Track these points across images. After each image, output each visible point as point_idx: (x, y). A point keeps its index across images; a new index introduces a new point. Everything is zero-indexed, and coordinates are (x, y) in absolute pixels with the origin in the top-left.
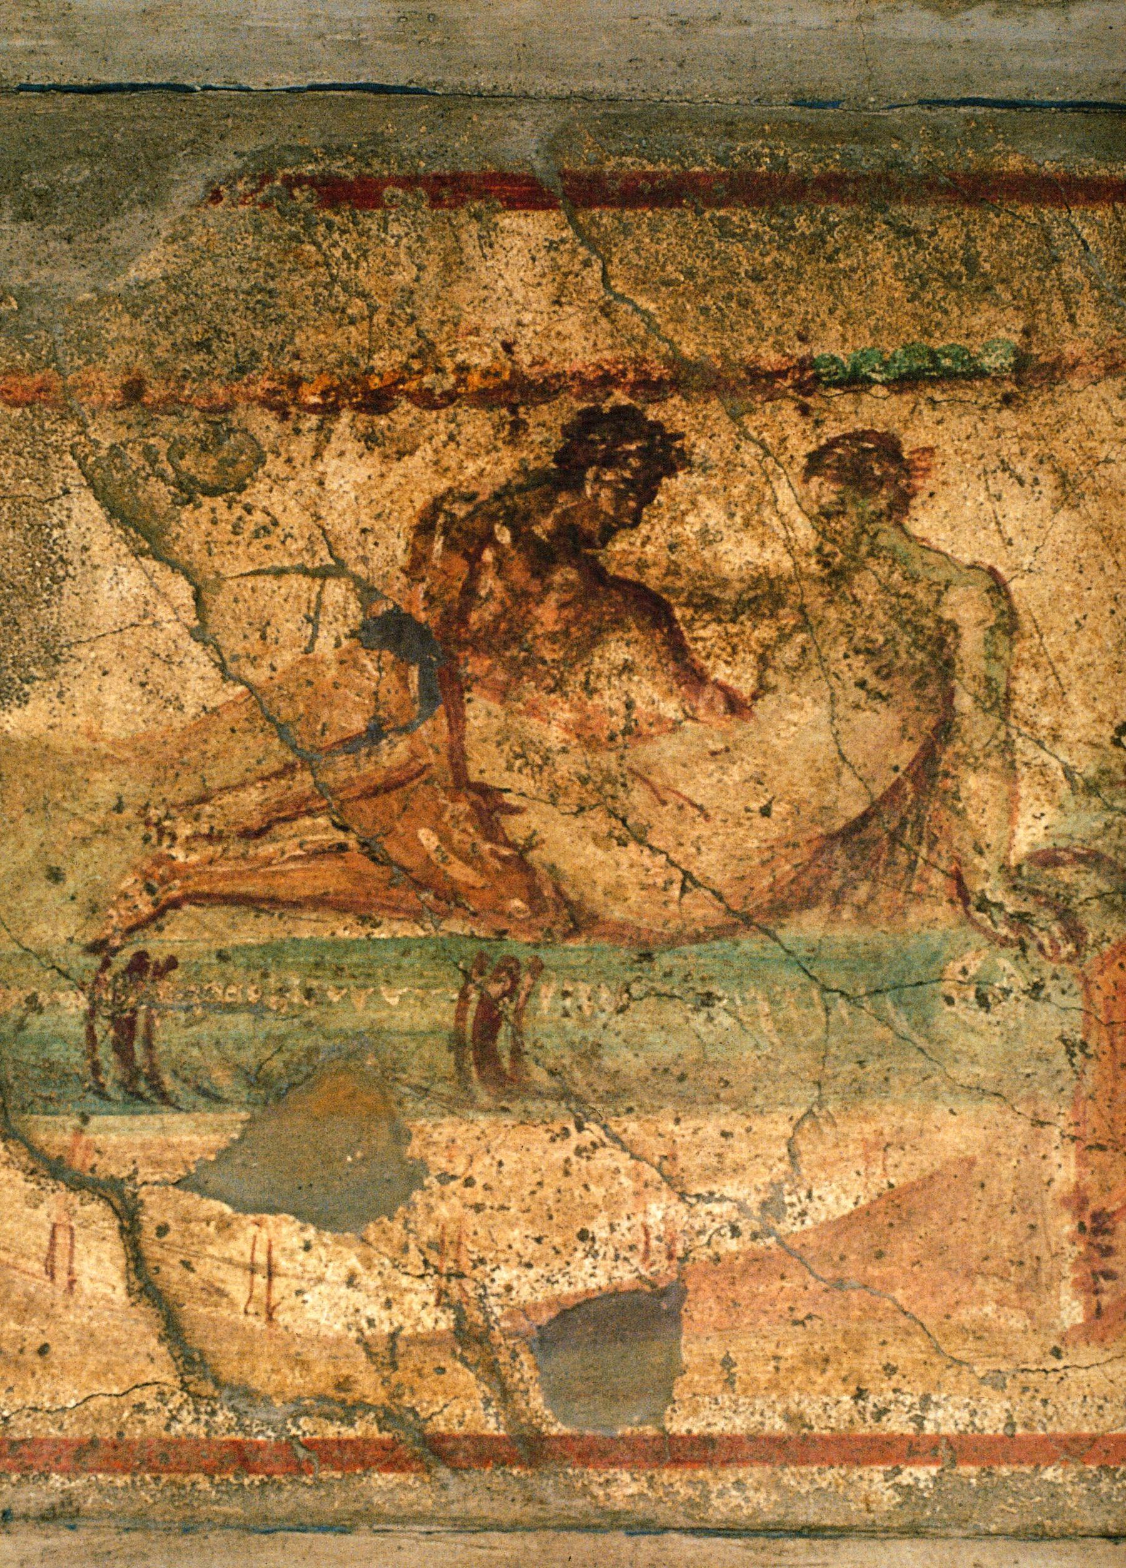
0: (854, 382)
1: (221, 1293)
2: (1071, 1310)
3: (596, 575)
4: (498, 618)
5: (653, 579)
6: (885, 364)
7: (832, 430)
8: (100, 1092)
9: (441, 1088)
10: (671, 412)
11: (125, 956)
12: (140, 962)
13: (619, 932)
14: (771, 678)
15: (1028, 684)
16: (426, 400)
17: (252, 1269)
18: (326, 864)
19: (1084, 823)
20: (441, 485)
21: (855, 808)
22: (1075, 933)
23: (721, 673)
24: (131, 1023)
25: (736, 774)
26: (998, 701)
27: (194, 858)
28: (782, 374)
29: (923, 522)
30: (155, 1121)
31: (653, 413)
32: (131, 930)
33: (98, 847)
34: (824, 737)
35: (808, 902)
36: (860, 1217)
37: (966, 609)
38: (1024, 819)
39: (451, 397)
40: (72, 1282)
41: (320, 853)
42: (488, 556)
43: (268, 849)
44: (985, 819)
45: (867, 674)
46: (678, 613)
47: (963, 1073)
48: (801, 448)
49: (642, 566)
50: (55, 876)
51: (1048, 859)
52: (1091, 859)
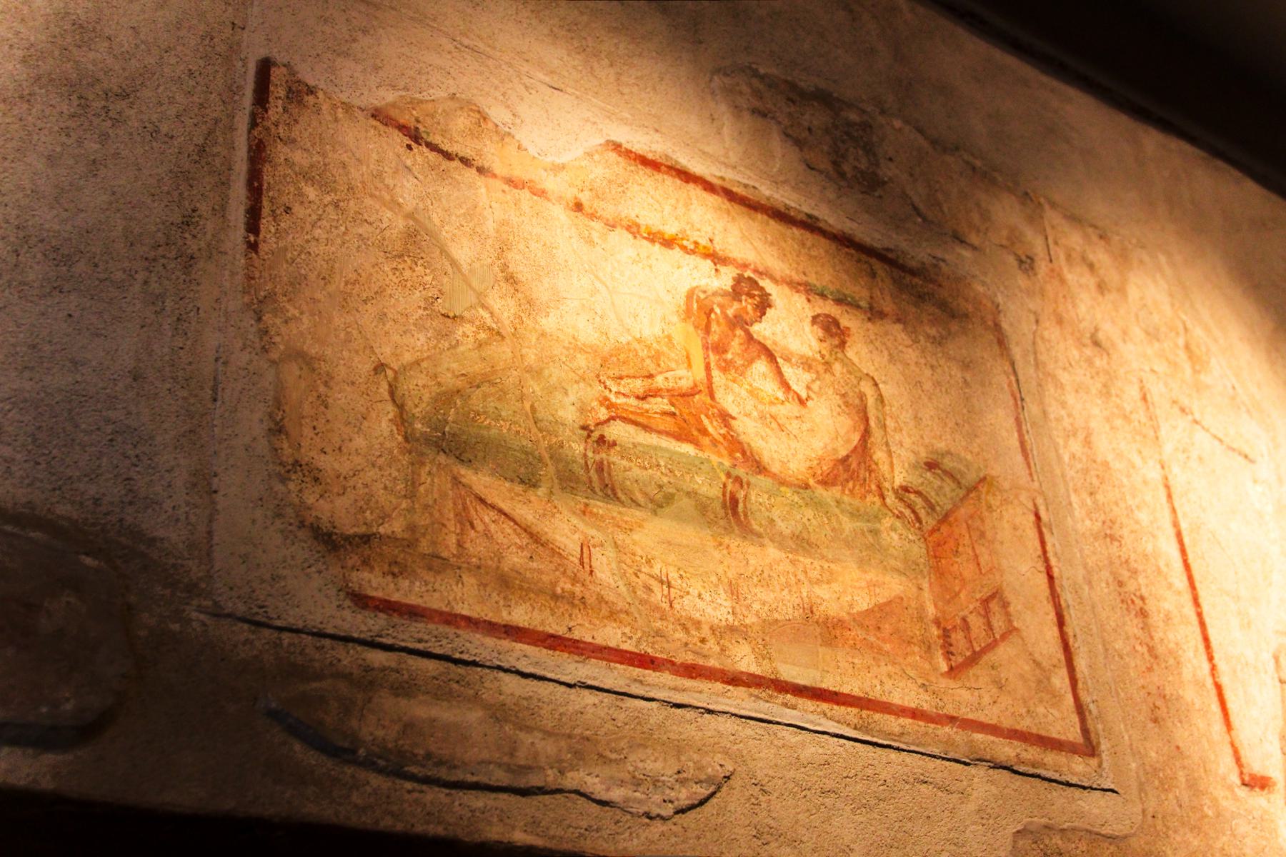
0: (823, 296)
1: (650, 590)
2: (944, 667)
3: (750, 337)
4: (720, 340)
5: (768, 343)
6: (832, 293)
7: (819, 311)
8: (593, 490)
9: (722, 523)
10: (766, 283)
11: (596, 435)
12: (602, 439)
13: (774, 476)
14: (811, 394)
15: (890, 423)
16: (684, 248)
17: (662, 582)
18: (668, 419)
19: (915, 480)
20: (695, 284)
21: (843, 453)
22: (918, 519)
23: (794, 387)
24: (602, 463)
25: (805, 427)
26: (884, 427)
27: (619, 401)
28: (799, 284)
29: (850, 353)
30: (616, 508)
31: (761, 283)
32: (597, 424)
33: (582, 385)
34: (830, 422)
35: (834, 484)
36: (869, 612)
37: (867, 388)
38: (896, 473)
39: (693, 252)
40: (592, 572)
41: (665, 413)
42: (713, 316)
43: (646, 406)
44: (884, 468)
45: (840, 402)
46: (779, 360)
47: (893, 562)
48: (810, 314)
49: (765, 338)
50: (566, 394)
51: (906, 489)
52: (918, 493)
